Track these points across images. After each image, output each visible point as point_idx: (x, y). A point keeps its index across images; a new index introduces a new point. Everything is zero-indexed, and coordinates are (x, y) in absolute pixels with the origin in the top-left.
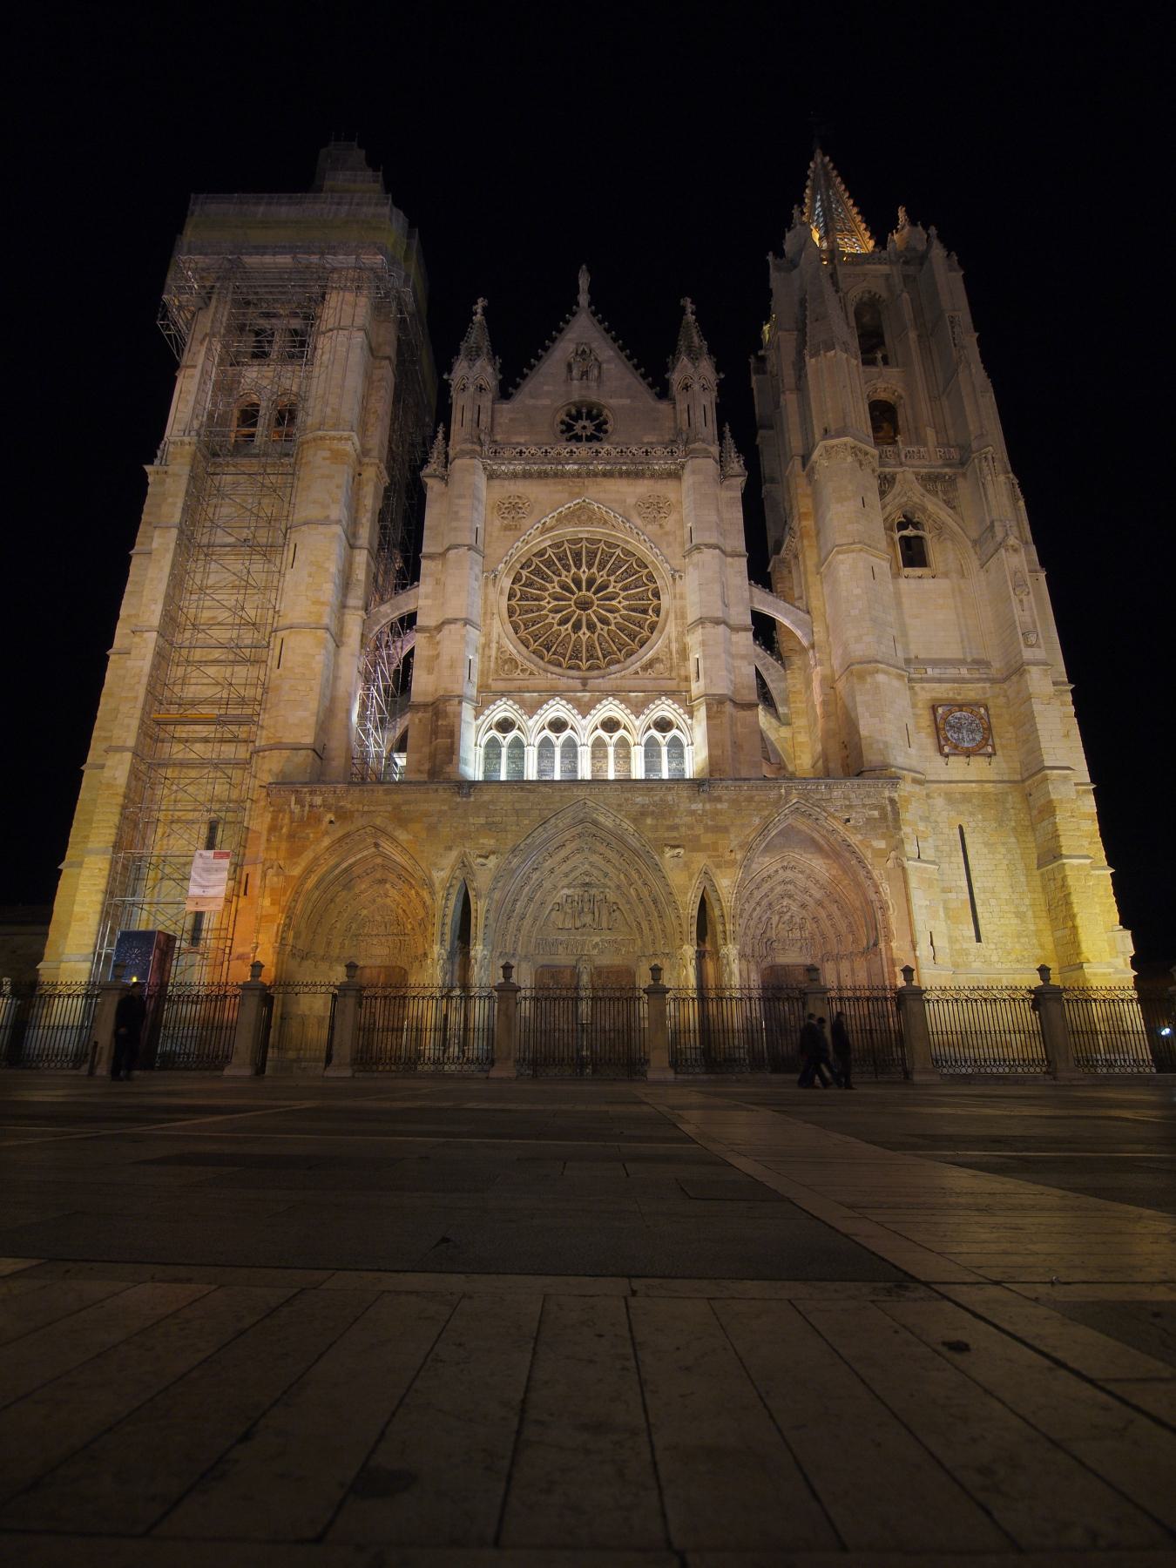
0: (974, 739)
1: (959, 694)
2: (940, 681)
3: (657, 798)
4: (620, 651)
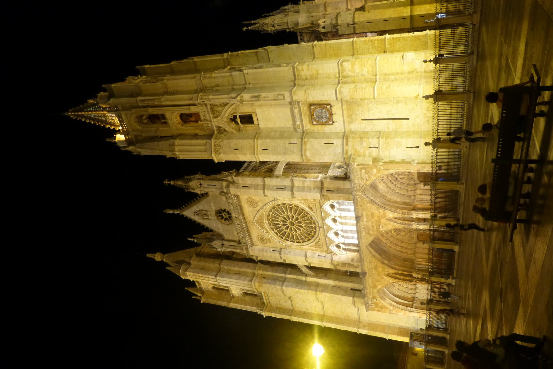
0: (325, 112)
1: (306, 114)
2: (302, 120)
3: (363, 230)
4: (307, 216)
